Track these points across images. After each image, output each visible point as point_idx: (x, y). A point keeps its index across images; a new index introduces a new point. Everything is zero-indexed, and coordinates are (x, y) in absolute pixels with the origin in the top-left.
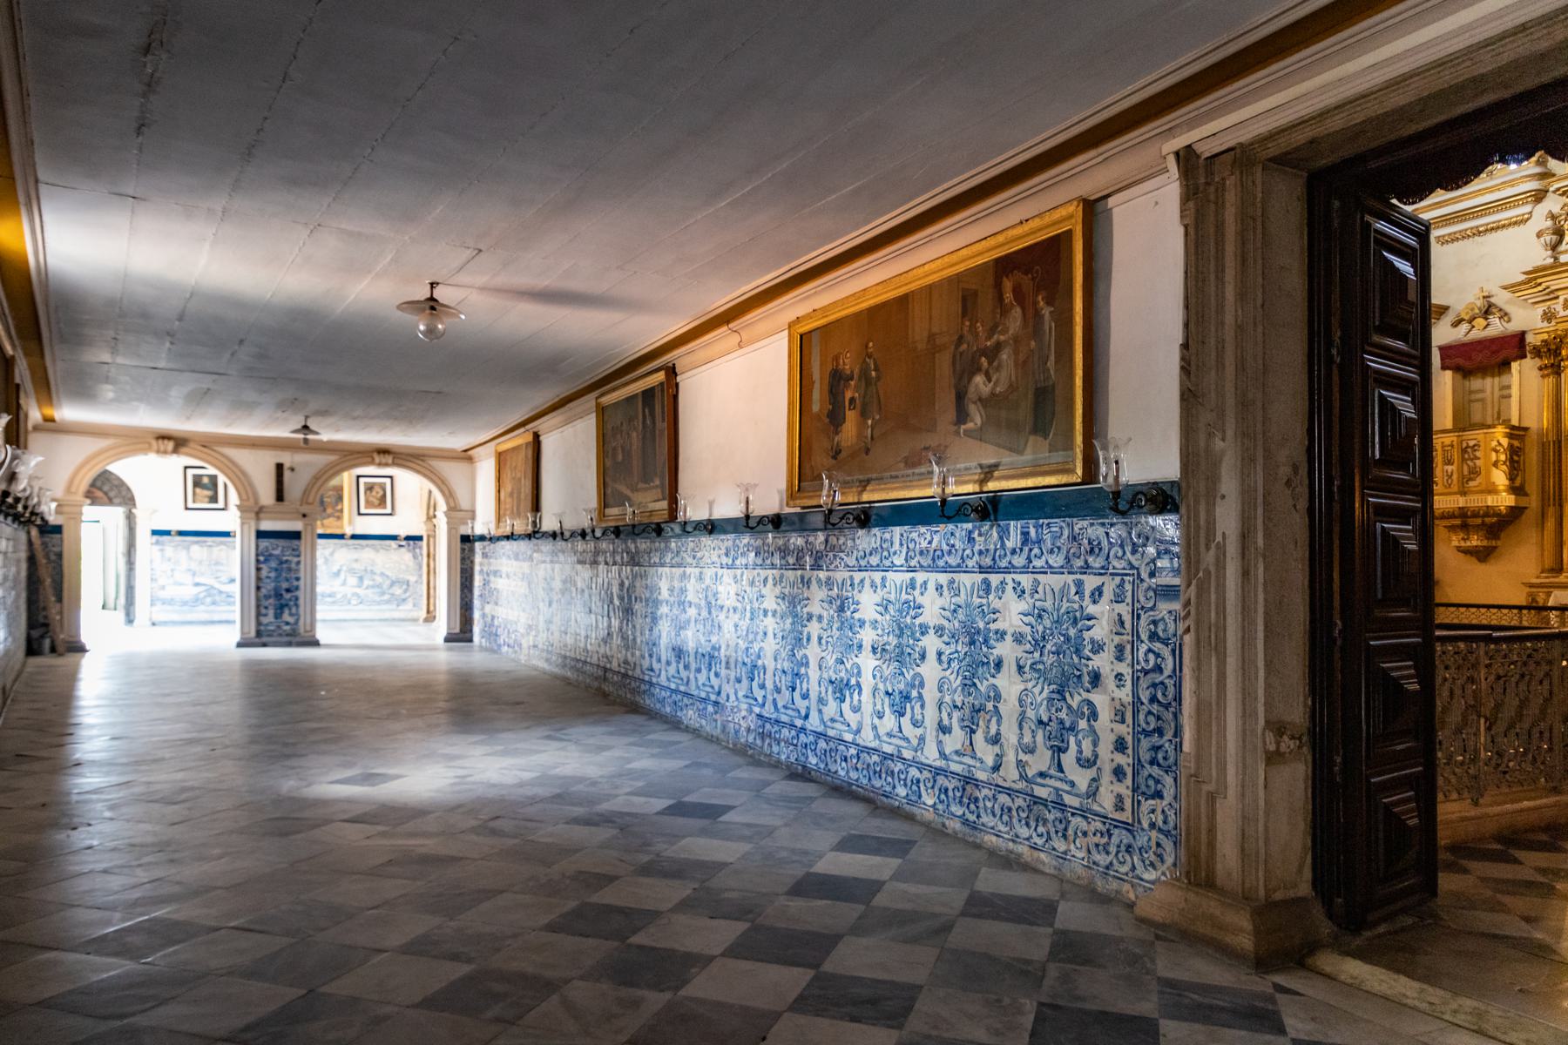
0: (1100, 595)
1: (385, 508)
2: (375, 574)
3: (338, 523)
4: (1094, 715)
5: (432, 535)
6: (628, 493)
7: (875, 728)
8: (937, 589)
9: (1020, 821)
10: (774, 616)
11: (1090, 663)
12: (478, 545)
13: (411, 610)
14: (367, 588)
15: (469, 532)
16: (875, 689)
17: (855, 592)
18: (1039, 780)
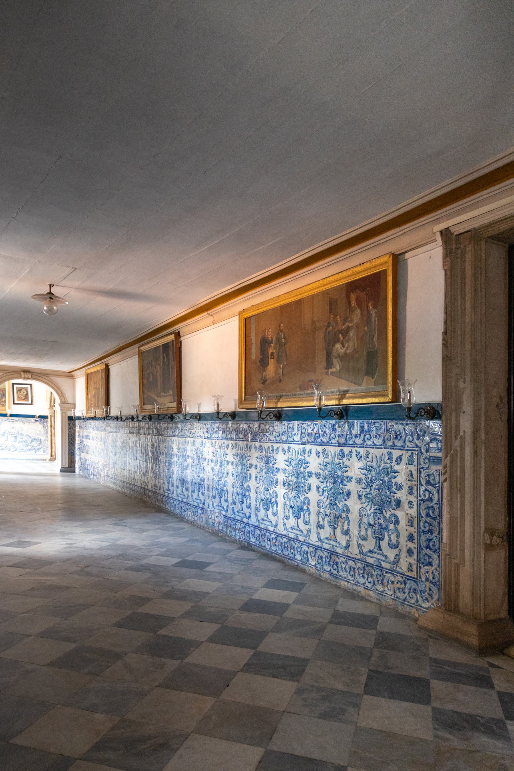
0: (401, 460)
1: (28, 401)
2: (23, 435)
3: (3, 408)
4: (397, 522)
5: (53, 416)
6: (156, 398)
7: (285, 524)
8: (317, 454)
9: (359, 575)
10: (232, 464)
11: (395, 495)
12: (77, 422)
13: (42, 455)
15: (73, 415)
16: (285, 505)
17: (275, 454)
18: (369, 554)
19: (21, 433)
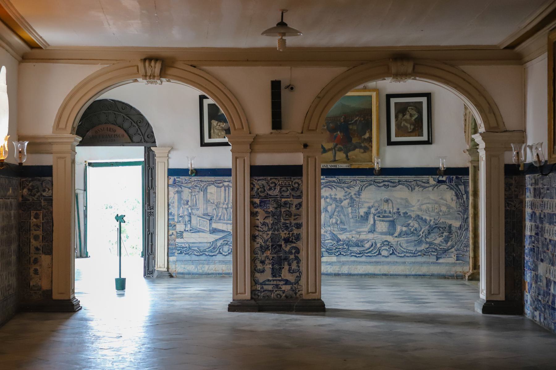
2: (410, 217)
3: (366, 155)
5: (476, 169)
12: (529, 179)
13: (454, 264)
14: (400, 235)
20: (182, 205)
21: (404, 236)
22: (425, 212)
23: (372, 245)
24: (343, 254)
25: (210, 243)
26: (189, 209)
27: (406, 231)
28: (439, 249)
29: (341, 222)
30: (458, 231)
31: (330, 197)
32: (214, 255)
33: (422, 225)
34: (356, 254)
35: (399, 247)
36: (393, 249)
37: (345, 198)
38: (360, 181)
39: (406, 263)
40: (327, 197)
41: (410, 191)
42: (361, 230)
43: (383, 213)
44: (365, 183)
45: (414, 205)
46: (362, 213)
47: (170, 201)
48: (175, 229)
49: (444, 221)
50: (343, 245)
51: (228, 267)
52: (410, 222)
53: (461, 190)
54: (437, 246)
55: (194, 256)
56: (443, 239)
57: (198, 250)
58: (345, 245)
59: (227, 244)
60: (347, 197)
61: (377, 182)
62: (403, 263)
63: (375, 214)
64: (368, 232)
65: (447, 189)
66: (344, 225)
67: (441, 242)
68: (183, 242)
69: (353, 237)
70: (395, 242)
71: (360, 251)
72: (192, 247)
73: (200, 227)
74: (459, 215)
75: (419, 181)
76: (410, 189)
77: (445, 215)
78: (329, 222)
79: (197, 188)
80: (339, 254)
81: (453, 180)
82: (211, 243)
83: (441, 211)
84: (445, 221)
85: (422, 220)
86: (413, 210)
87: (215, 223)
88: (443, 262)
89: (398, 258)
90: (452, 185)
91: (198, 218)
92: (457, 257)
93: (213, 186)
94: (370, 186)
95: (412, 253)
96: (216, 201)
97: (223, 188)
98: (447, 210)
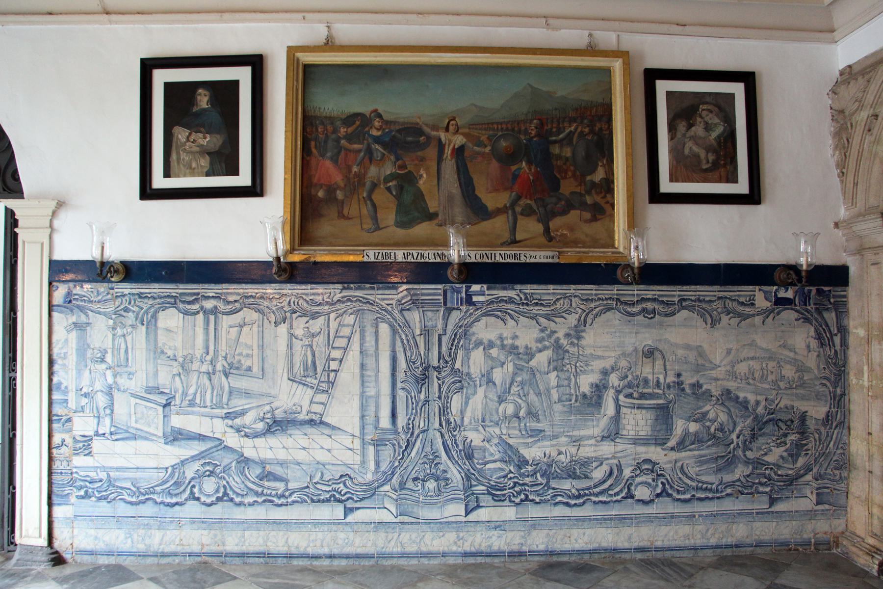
1: (732, 178)
2: (708, 395)
3: (596, 229)
13: (810, 515)
14: (681, 445)
19: (697, 386)
20: (89, 362)
21: (693, 446)
22: (744, 381)
23: (611, 473)
24: (533, 500)
25: (167, 469)
26: (109, 373)
27: (697, 432)
28: (776, 477)
29: (529, 413)
30: (822, 429)
31: (498, 342)
32: (177, 504)
33: (737, 416)
34: (570, 497)
35: (680, 475)
36: (664, 481)
37: (540, 346)
38: (583, 300)
39: (694, 516)
40: (491, 345)
41: (709, 326)
42: (583, 433)
43: (641, 387)
44: (593, 305)
45: (718, 363)
46: (585, 388)
47: (56, 351)
48: (71, 430)
49: (789, 403)
50: (535, 473)
51: (215, 536)
52: (707, 408)
53: (830, 325)
54: (771, 469)
55: (122, 504)
56: (786, 451)
57: (134, 489)
58: (538, 475)
59: (212, 473)
60: (547, 343)
61: (626, 303)
62: (687, 516)
63: (618, 389)
64: (599, 439)
65: (796, 320)
66: (538, 420)
67: (782, 457)
68: (91, 464)
69: (560, 453)
70: (670, 462)
71: (578, 490)
72: (116, 480)
73: (138, 426)
74: (824, 389)
75: (729, 298)
76: (709, 320)
77: (791, 388)
78: (498, 413)
79: (131, 314)
80: (522, 500)
81: (810, 299)
82: (170, 470)
83: (783, 377)
84: (792, 403)
85: (737, 402)
86: (715, 376)
87: (177, 414)
88: (785, 510)
89: (676, 504)
90: (807, 310)
91: (133, 401)
92: (817, 493)
93: (173, 311)
94: (608, 313)
95: (710, 490)
96: (180, 354)
97: (201, 316)
98: (797, 374)
